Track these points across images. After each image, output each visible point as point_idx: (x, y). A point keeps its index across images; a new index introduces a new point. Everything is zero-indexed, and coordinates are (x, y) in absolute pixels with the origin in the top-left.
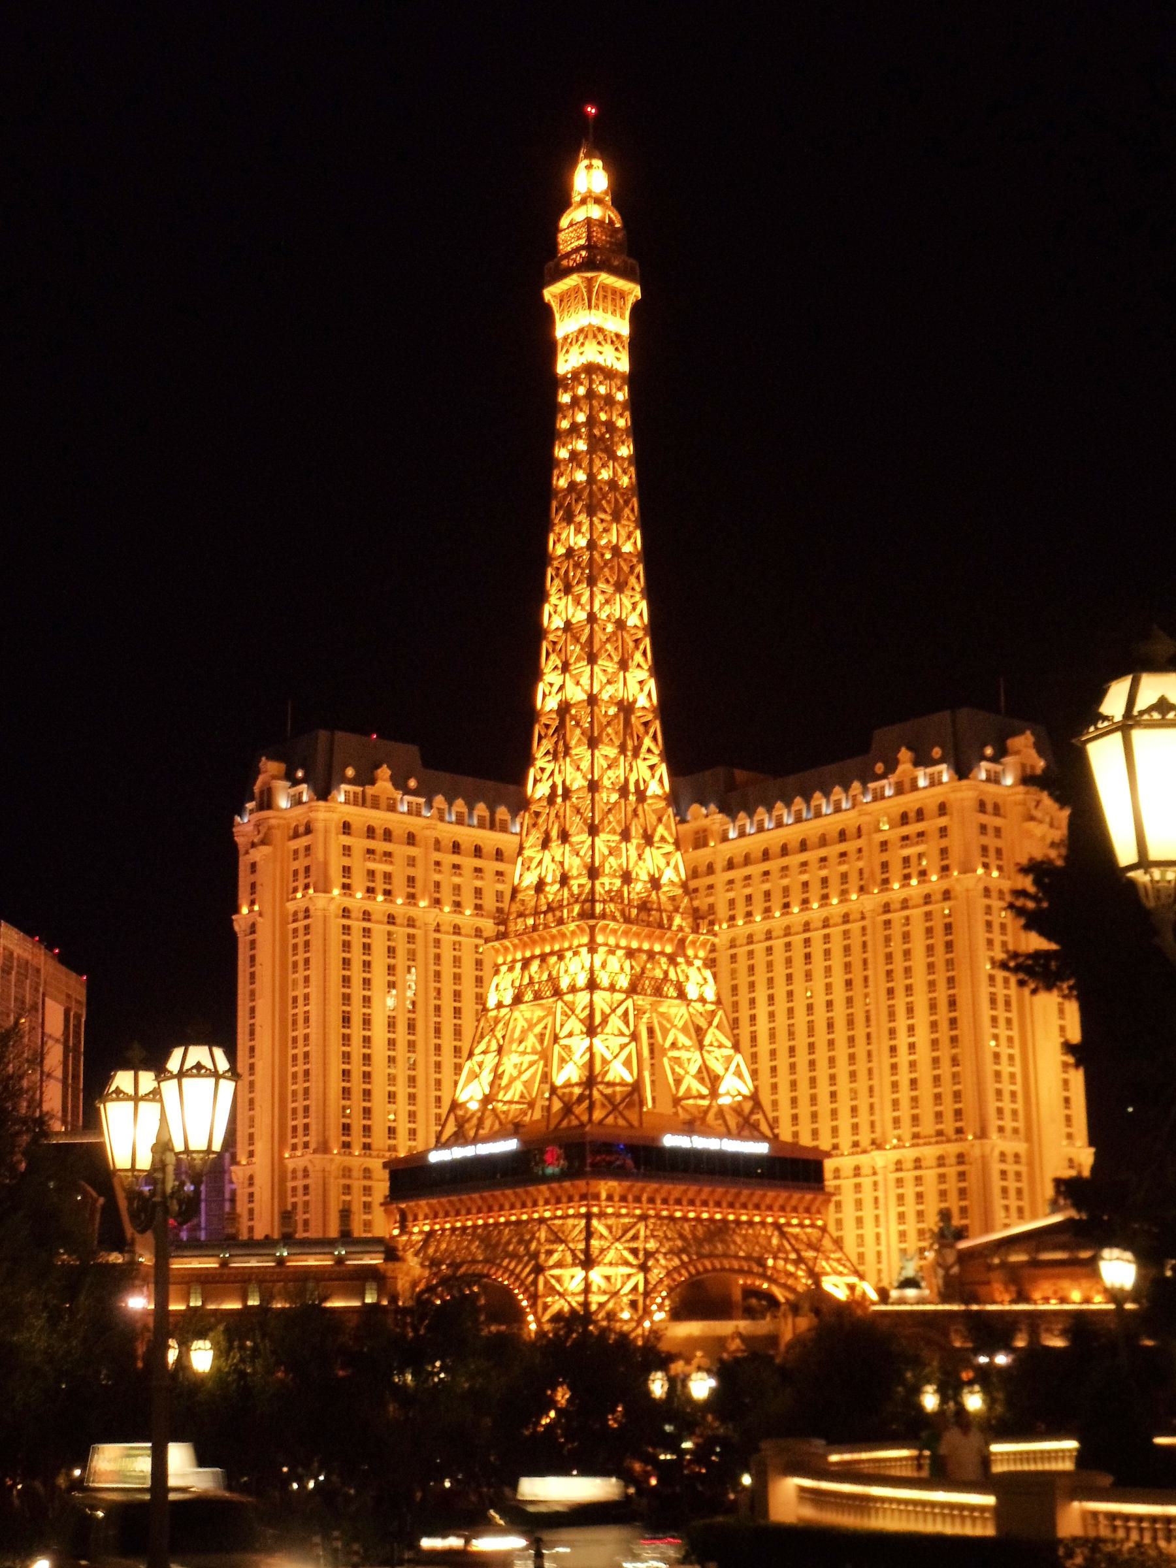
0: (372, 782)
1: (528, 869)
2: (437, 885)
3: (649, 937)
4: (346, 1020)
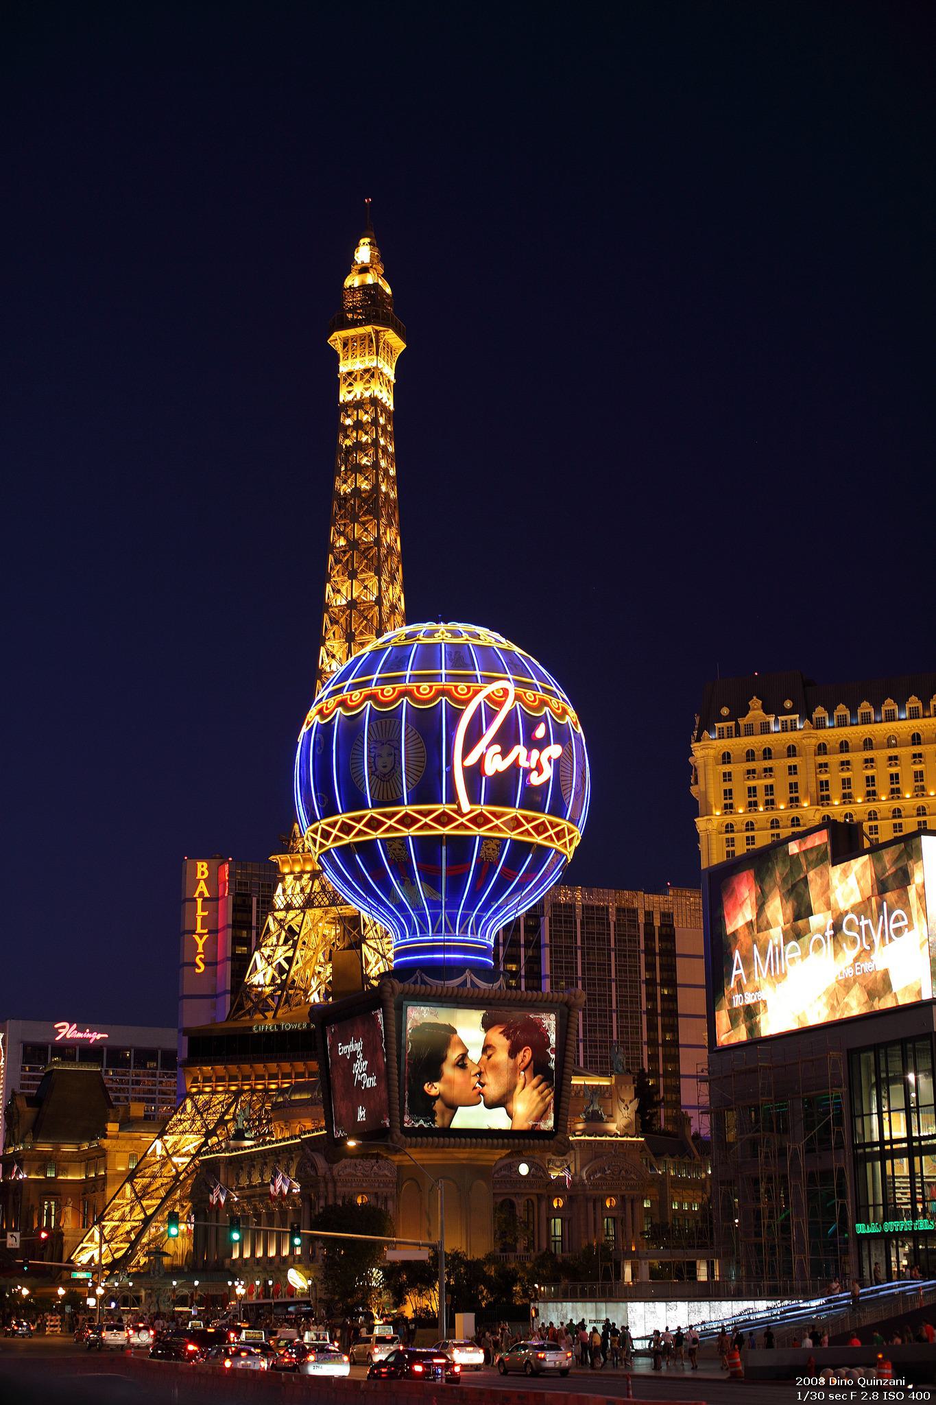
0: (745, 711)
2: (824, 785)
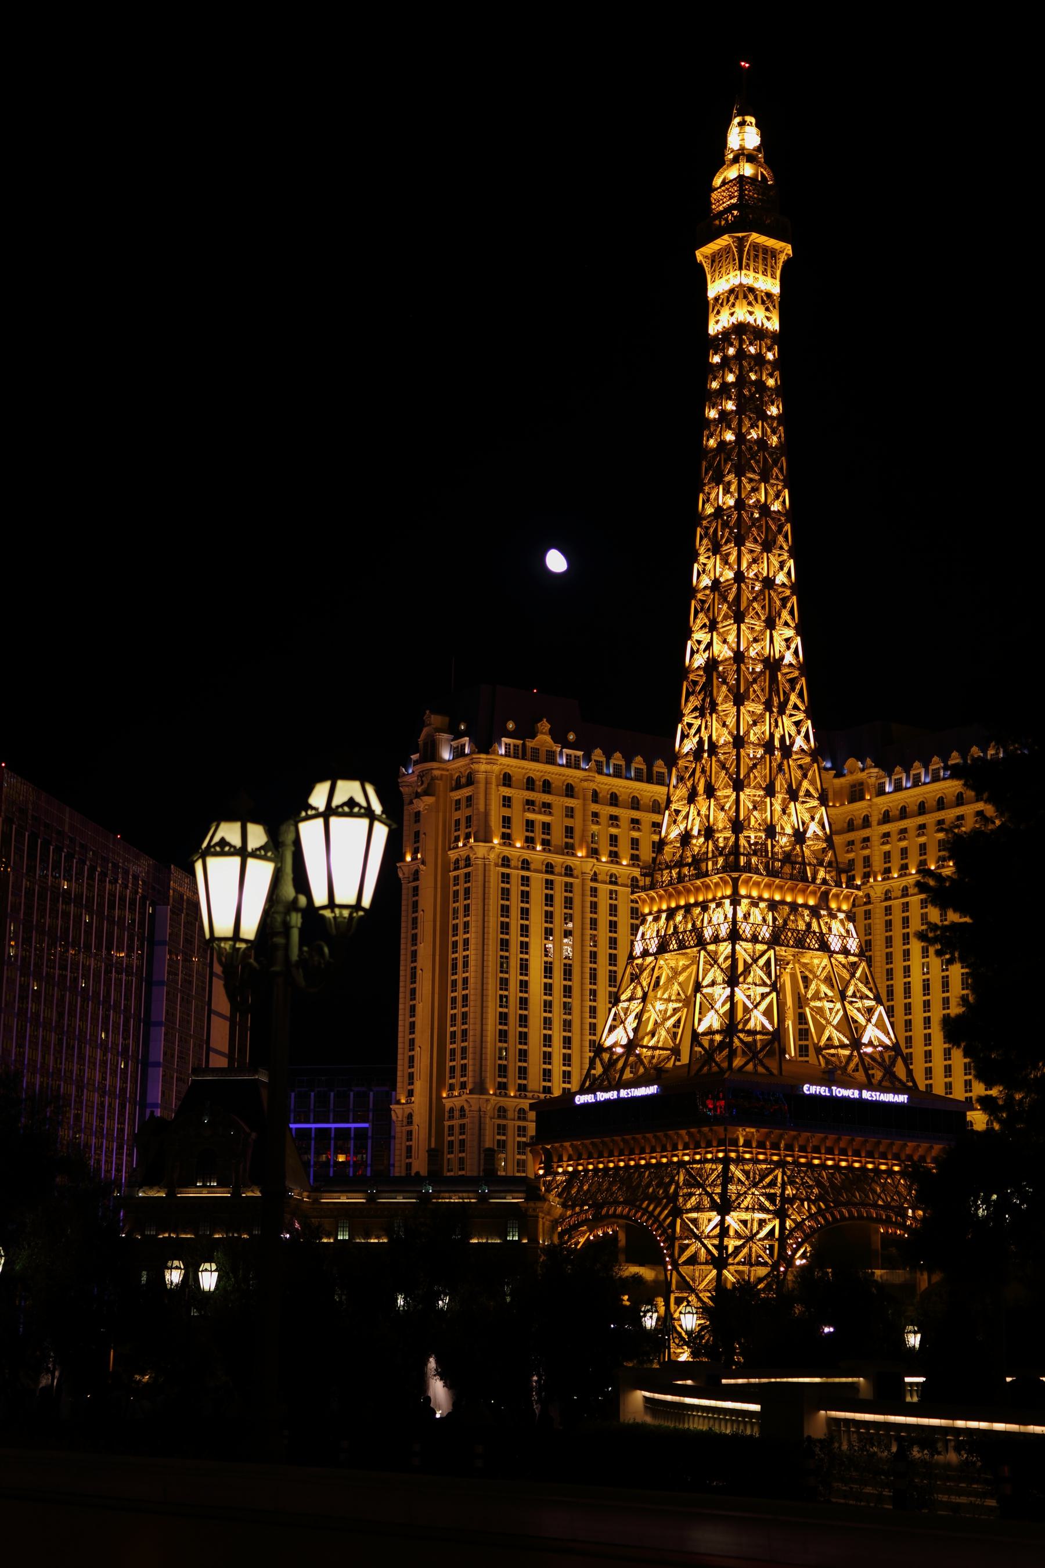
1: (675, 822)
3: (792, 890)
4: (504, 965)
